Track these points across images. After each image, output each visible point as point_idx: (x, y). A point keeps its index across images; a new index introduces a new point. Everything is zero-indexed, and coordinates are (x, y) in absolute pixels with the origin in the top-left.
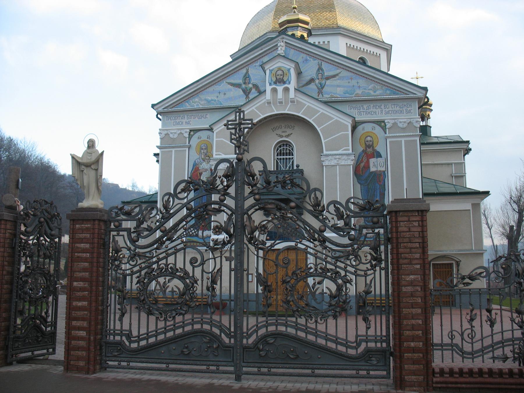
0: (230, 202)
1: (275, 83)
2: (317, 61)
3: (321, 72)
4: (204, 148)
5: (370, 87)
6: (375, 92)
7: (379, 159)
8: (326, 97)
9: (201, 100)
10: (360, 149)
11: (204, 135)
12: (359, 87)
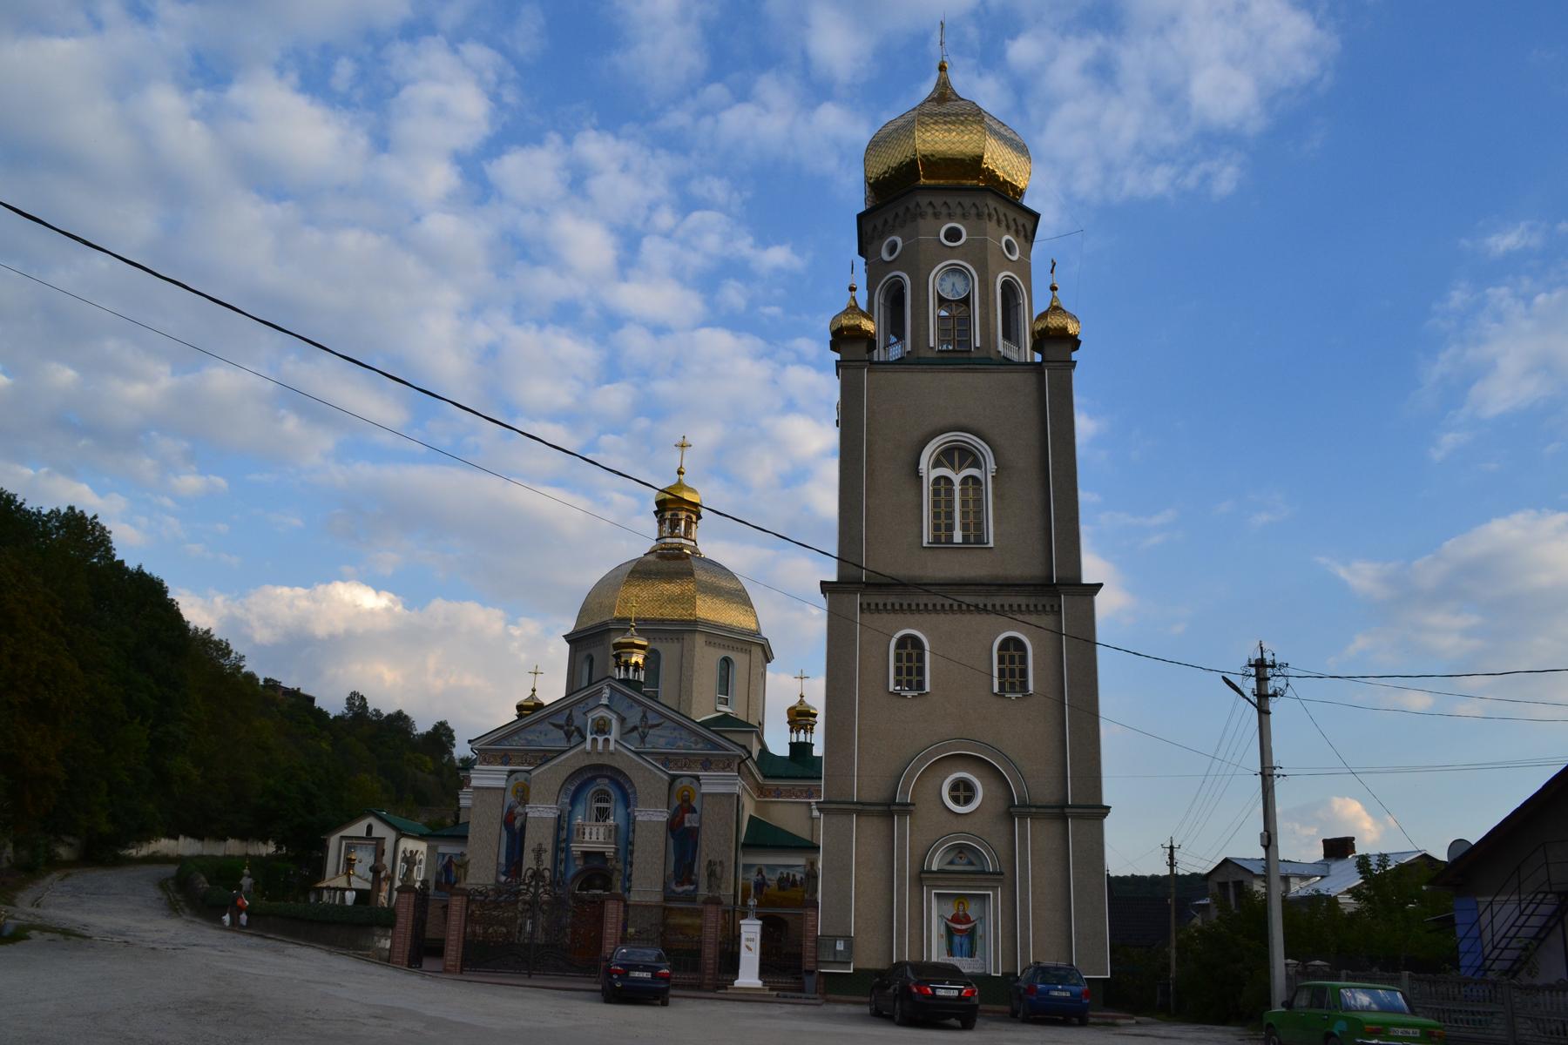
0: (532, 889)
1: (596, 733)
2: (641, 709)
5: (693, 739)
7: (695, 815)
8: (648, 748)
9: (520, 738)
10: (676, 803)
12: (681, 739)
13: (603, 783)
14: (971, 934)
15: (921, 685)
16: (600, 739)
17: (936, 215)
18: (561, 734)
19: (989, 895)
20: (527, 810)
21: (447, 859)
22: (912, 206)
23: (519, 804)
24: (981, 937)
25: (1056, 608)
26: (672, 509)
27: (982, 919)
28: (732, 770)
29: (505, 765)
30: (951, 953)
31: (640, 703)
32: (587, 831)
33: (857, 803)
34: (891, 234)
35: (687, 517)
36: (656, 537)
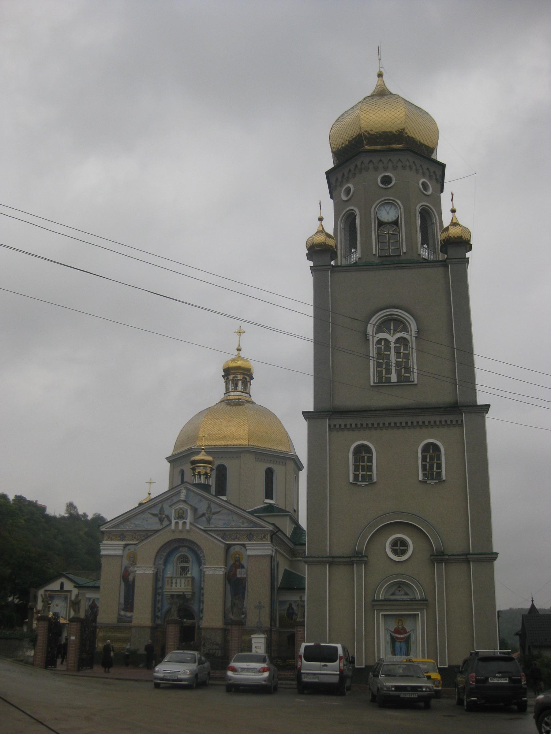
1: (178, 518)
3: (209, 509)
4: (132, 556)
5: (240, 521)
6: (243, 524)
7: (243, 569)
8: (212, 527)
10: (231, 562)
11: (132, 548)
12: (233, 520)
13: (184, 551)
14: (407, 641)
15: (371, 477)
16: (181, 522)
17: (376, 169)
18: (156, 520)
19: (418, 614)
20: (136, 569)
21: (91, 601)
22: (359, 164)
23: (132, 565)
24: (414, 642)
25: (460, 422)
26: (233, 374)
27: (414, 630)
28: (267, 540)
29: (122, 541)
30: (394, 653)
31: (207, 499)
32: (174, 581)
33: (329, 557)
34: (348, 181)
35: (244, 378)
36: (224, 393)
